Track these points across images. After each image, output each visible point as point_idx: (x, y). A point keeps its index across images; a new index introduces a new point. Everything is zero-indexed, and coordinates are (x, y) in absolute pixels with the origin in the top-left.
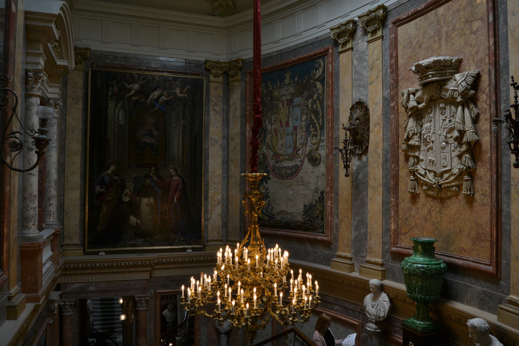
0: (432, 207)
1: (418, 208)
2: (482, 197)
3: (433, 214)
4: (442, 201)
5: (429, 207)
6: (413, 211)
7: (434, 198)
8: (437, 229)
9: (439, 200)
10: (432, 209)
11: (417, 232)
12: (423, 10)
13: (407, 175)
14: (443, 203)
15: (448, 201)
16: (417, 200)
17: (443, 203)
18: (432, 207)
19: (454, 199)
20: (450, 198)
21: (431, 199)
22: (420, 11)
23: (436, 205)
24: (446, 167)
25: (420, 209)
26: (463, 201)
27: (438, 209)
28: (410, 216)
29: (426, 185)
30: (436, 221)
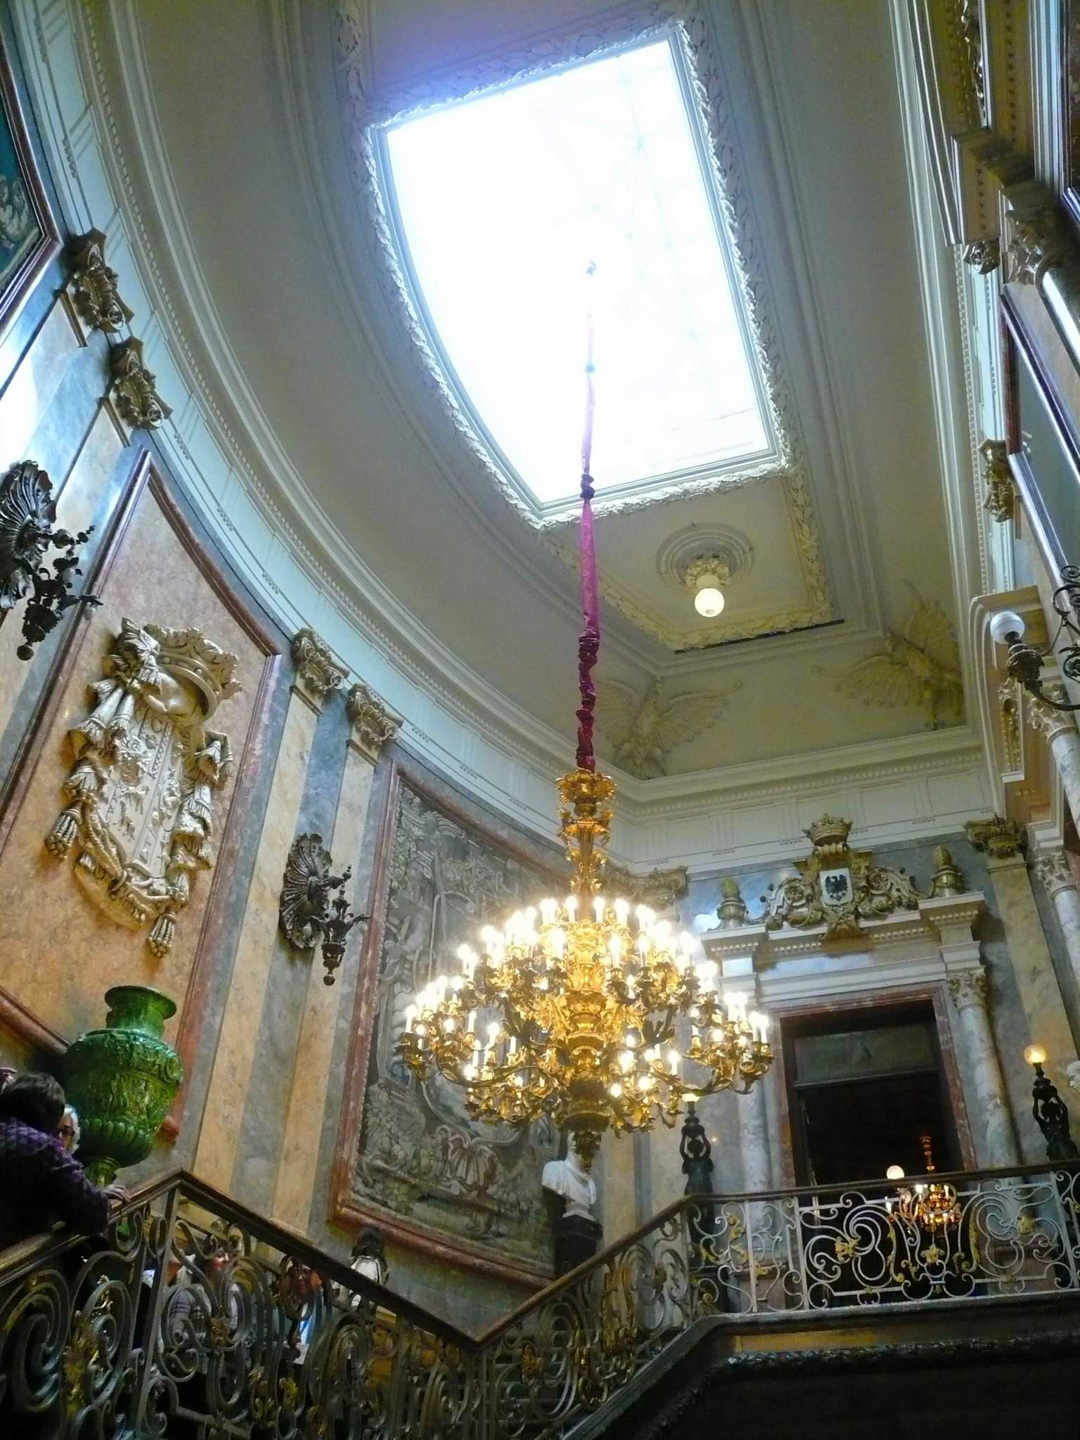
0: (78, 917)
1: (45, 895)
2: (175, 971)
3: (75, 936)
4: (101, 918)
5: (70, 913)
6: (33, 892)
7: (88, 900)
8: (71, 978)
9: (95, 913)
10: (76, 922)
11: (24, 954)
12: (192, 541)
13: (51, 791)
14: (100, 927)
15: (112, 929)
16: (50, 874)
17: (100, 927)
18: (76, 916)
19: (122, 937)
20: (118, 927)
21: (78, 898)
22: (188, 533)
23: (85, 921)
24: (145, 861)
25: (48, 901)
26: (139, 954)
27: (86, 933)
28: (21, 897)
29: (94, 862)
30: (75, 958)
